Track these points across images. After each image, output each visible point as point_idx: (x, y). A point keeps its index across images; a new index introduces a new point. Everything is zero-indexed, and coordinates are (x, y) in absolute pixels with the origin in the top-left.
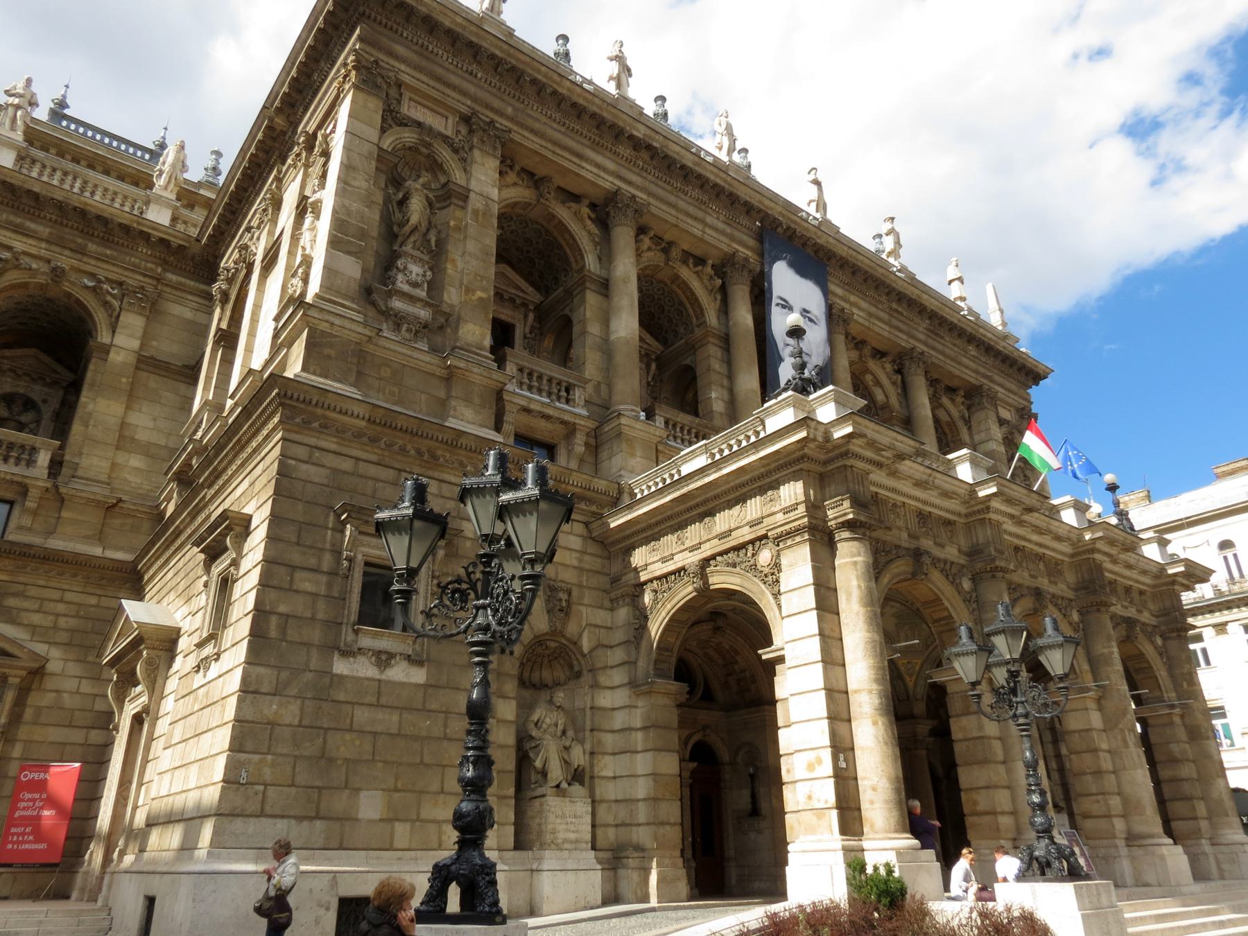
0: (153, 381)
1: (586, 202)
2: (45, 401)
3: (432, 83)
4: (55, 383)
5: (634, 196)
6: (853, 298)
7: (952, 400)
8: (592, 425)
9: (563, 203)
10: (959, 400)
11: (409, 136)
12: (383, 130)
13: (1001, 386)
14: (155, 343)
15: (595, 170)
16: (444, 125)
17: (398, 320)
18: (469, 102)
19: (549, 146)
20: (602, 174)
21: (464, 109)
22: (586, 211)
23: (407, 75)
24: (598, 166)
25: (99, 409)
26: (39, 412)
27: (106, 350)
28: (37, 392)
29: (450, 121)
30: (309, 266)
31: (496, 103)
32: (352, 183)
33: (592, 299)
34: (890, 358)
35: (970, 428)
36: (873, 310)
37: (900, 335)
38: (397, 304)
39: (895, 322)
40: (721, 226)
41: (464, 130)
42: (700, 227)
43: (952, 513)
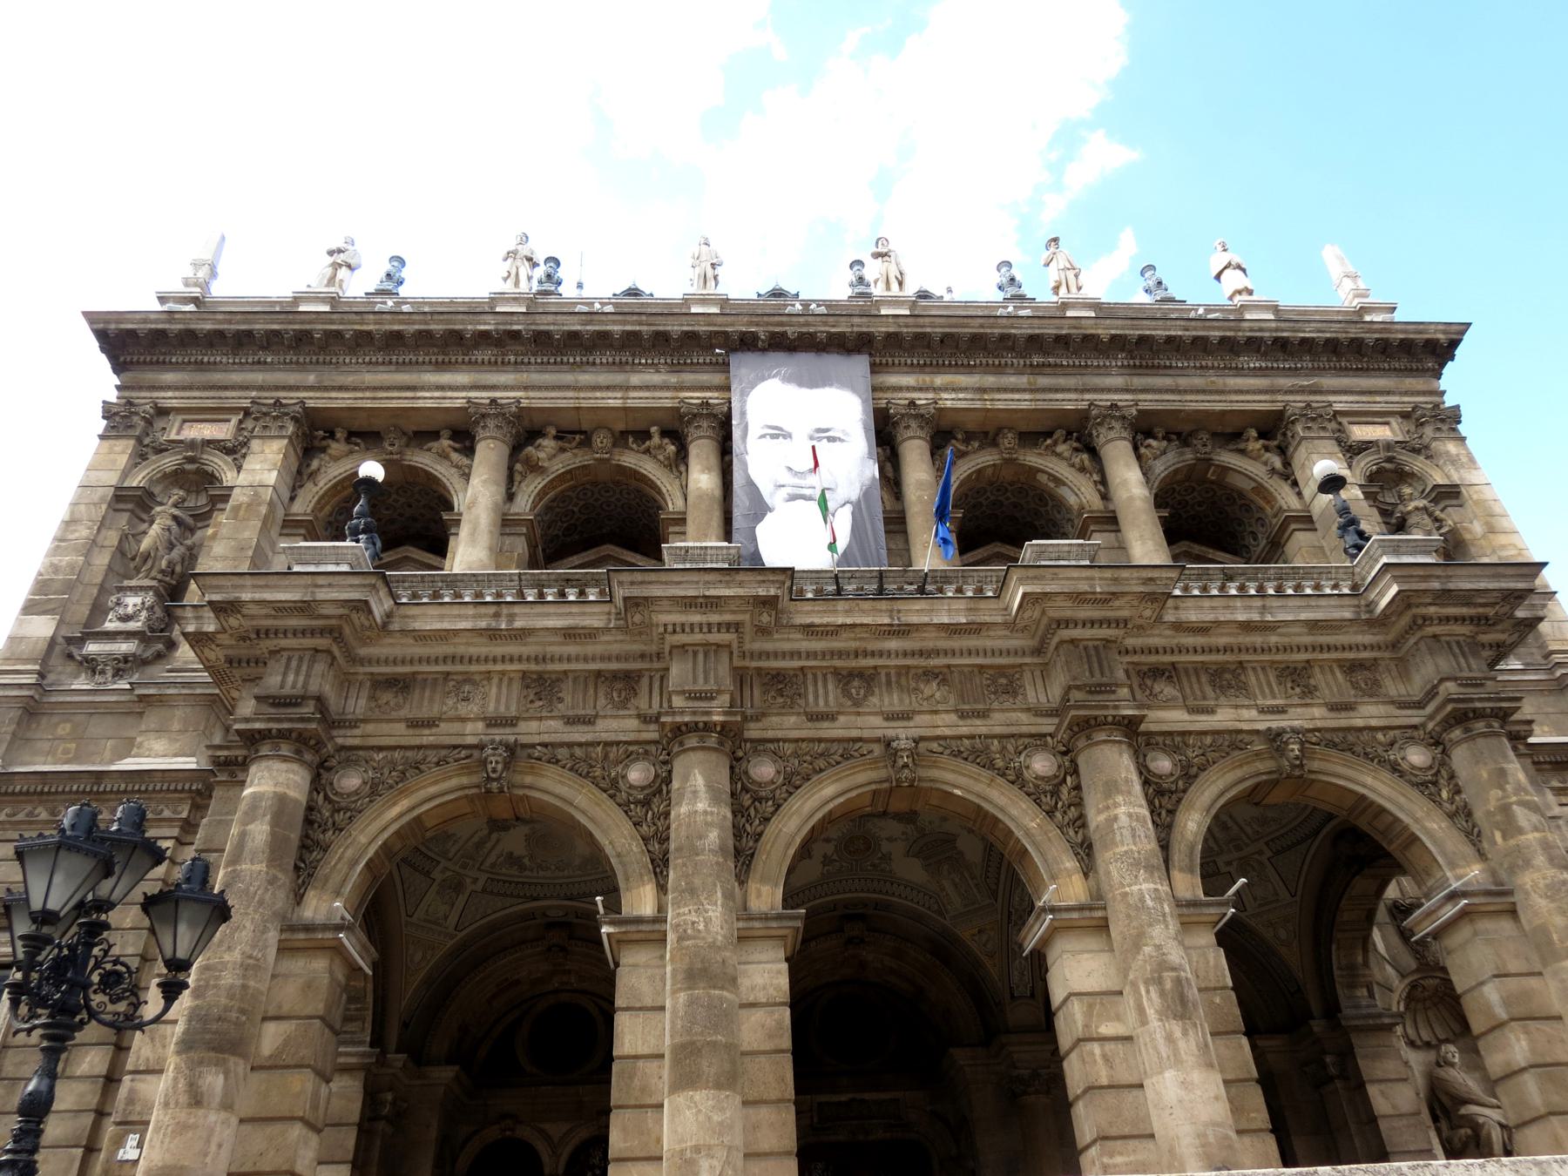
5: (493, 401)
6: (939, 380)
7: (1243, 452)
10: (1255, 446)
11: (169, 462)
13: (1341, 391)
15: (437, 394)
17: (91, 665)
19: (368, 394)
20: (449, 394)
21: (246, 403)
22: (446, 443)
23: (169, 399)
34: (1059, 434)
35: (1295, 484)
36: (990, 380)
37: (1059, 396)
38: (92, 648)
39: (1043, 381)
42: (619, 395)
43: (626, 657)
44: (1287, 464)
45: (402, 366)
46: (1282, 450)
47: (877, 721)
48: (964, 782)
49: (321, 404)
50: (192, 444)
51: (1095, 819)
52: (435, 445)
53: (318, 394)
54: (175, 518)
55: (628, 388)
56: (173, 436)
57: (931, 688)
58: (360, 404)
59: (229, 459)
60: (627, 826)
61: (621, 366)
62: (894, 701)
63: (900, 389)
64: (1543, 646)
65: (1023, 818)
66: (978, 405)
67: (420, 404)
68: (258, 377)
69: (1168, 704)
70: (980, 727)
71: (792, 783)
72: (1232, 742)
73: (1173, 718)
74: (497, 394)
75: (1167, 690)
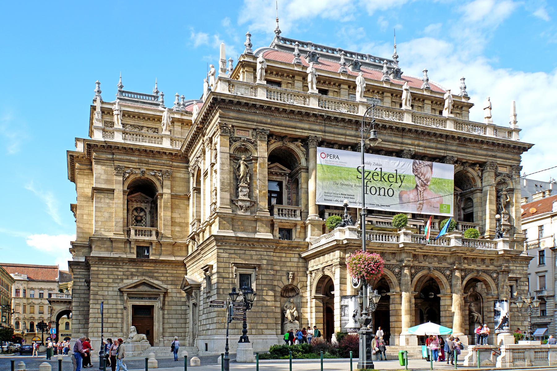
0: (177, 202)
1: (300, 140)
2: (146, 208)
3: (243, 122)
4: (147, 202)
6: (416, 142)
7: (474, 169)
8: (302, 222)
9: (292, 142)
10: (477, 168)
11: (237, 144)
12: (230, 145)
14: (175, 189)
15: (301, 131)
16: (249, 135)
18: (255, 124)
19: (284, 128)
20: (304, 131)
21: (254, 127)
22: (300, 144)
24: (302, 129)
25: (163, 214)
26: (145, 212)
27: (162, 195)
28: (143, 206)
29: (250, 132)
30: (216, 190)
31: (264, 120)
32: (224, 169)
33: (303, 175)
35: (482, 180)
36: (427, 144)
37: (441, 151)
39: (439, 146)
40: (353, 133)
41: (255, 134)
44: (482, 174)
45: (291, 120)
46: (482, 171)
47: (427, 263)
48: (437, 274)
49: (272, 130)
50: (244, 141)
51: (454, 282)
52: (296, 143)
53: (271, 126)
54: (246, 165)
55: (346, 135)
56: (236, 136)
57: (436, 259)
58: (282, 131)
59: (252, 145)
60: (395, 278)
61: (344, 127)
62: (430, 260)
63: (407, 144)
64: (514, 231)
65: (444, 280)
66: (423, 151)
67: (297, 133)
68: (256, 118)
69: (466, 264)
70: (441, 266)
71: (416, 273)
72: (472, 270)
73: (466, 266)
74: (316, 133)
75: (466, 261)
